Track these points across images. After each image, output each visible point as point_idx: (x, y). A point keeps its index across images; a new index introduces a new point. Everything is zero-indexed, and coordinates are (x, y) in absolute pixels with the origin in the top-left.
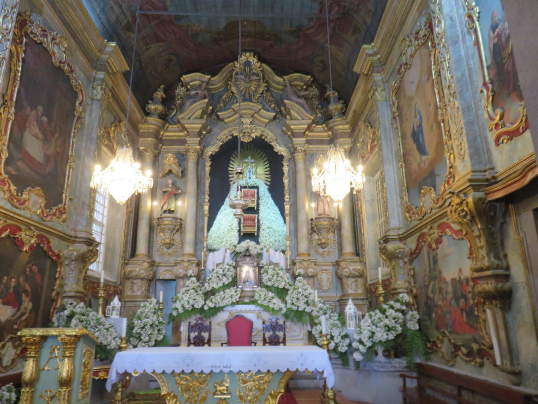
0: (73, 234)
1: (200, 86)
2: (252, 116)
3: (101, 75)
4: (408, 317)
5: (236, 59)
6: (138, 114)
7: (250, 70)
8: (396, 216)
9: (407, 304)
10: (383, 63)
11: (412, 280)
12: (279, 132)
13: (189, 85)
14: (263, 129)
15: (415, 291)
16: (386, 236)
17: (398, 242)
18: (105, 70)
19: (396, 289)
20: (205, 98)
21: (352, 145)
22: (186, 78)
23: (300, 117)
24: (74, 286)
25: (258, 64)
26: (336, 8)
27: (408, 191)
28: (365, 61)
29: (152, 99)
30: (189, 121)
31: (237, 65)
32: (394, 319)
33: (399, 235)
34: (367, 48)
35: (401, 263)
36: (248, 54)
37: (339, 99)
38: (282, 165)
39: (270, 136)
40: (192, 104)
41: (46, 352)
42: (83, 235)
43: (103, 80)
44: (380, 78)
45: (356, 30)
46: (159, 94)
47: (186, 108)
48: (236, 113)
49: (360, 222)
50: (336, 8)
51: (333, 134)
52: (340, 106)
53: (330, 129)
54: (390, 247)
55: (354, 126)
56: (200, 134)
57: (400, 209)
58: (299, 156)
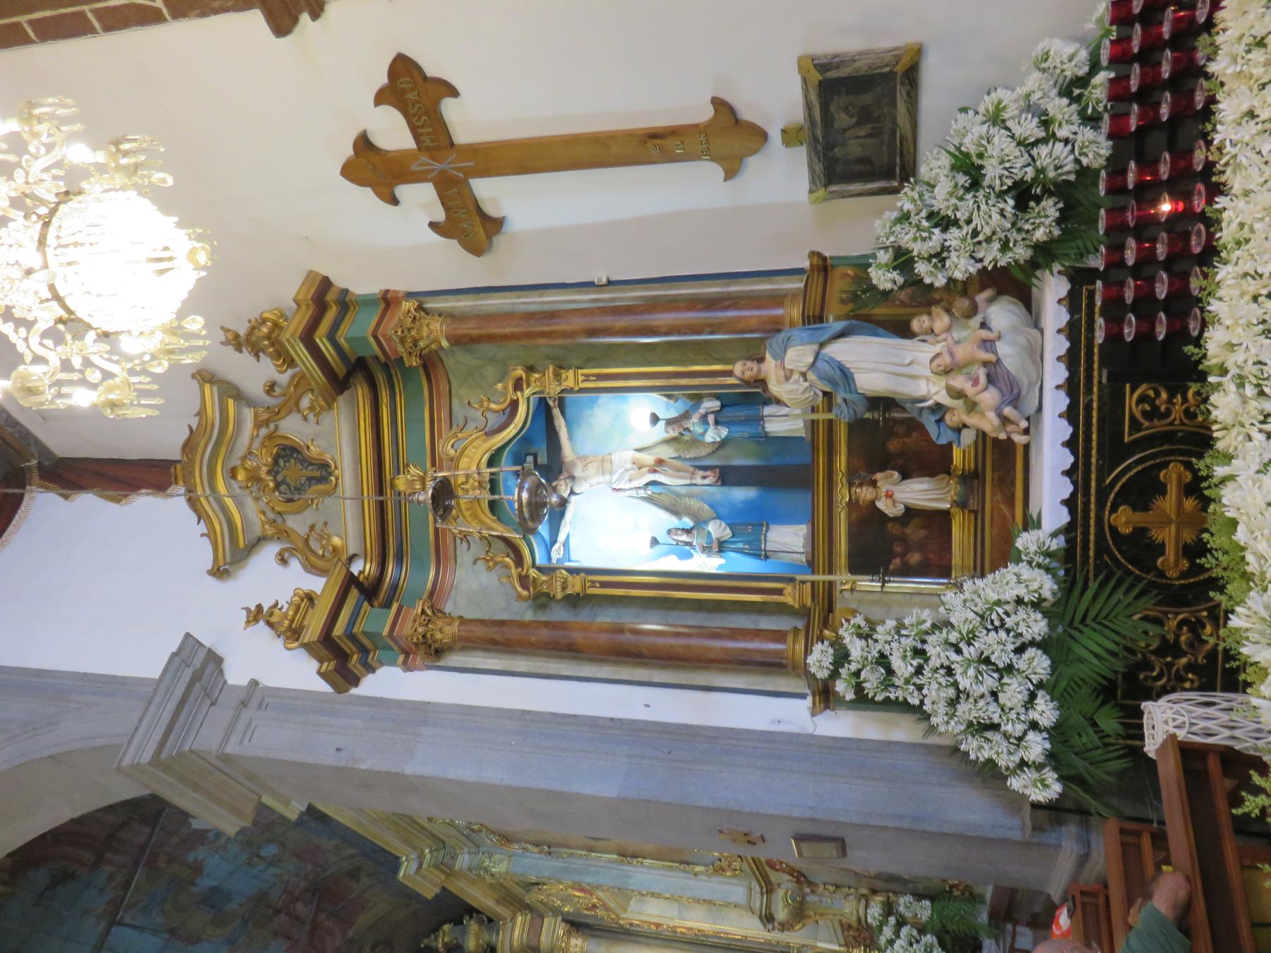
4: (908, 915)
8: (726, 887)
9: (889, 909)
10: (440, 843)
11: (846, 890)
15: (864, 891)
16: (761, 918)
17: (774, 896)
19: (859, 920)
21: (560, 918)
26: (300, 908)
27: (688, 863)
28: (424, 877)
32: (911, 945)
33: (762, 894)
34: (406, 871)
35: (811, 898)
37: (458, 922)
44: (467, 856)
45: (354, 874)
49: (719, 938)
50: (300, 908)
52: (473, 927)
54: (781, 914)
55: (529, 908)
57: (715, 879)
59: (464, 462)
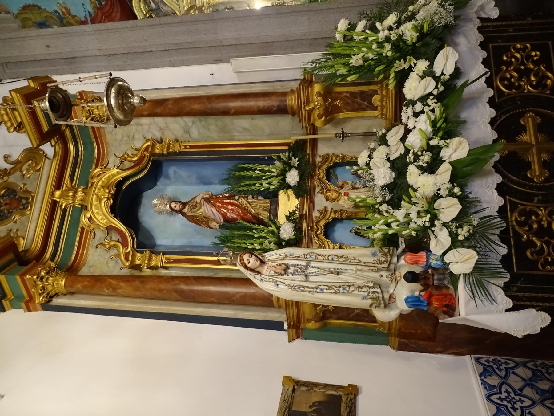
13: (146, 15)
30: (181, 4)
40: (165, 4)
47: (170, 9)
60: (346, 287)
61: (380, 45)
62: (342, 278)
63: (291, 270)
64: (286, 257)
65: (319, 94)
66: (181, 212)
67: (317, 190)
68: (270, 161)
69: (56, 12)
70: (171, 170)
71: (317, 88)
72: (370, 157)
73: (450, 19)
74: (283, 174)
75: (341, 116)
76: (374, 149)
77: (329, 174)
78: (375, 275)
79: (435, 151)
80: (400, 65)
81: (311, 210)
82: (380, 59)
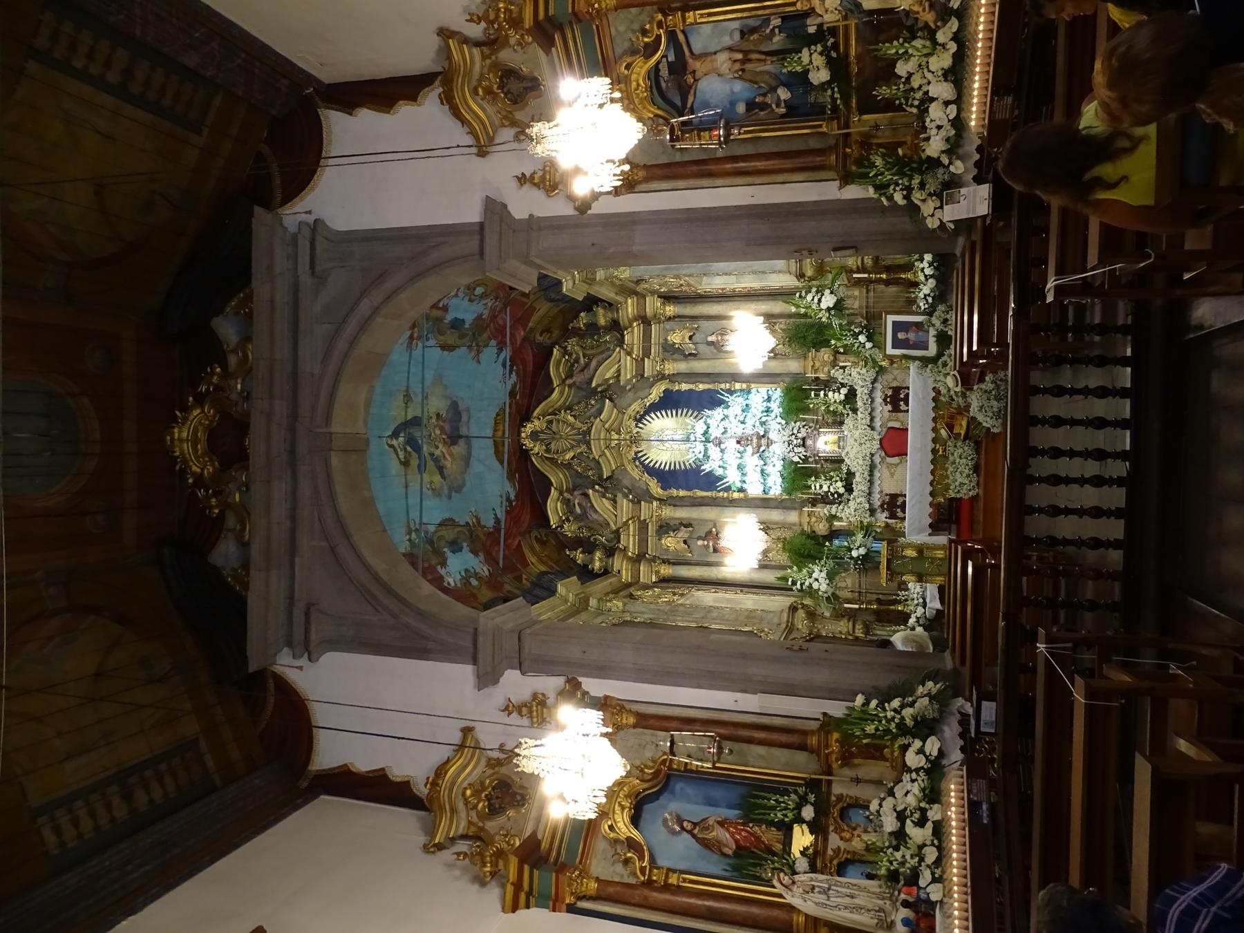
0: (784, 626)
1: (567, 502)
2: (607, 430)
3: (593, 602)
5: (527, 451)
6: (613, 579)
7: (542, 432)
12: (631, 394)
14: (626, 417)
18: (587, 601)
20: (586, 495)
22: (553, 522)
23: (618, 366)
24: (842, 623)
25: (536, 422)
29: (586, 566)
31: (536, 450)
34: (566, 288)
36: (523, 435)
38: (679, 391)
39: (636, 407)
40: (596, 511)
41: (898, 570)
42: (785, 616)
43: (600, 600)
46: (580, 557)
48: (603, 454)
51: (636, 319)
52: (601, 311)
53: (631, 326)
54: (809, 272)
55: (636, 293)
56: (637, 502)
58: (670, 368)
59: (634, 77)
60: (859, 909)
61: (888, 721)
62: (856, 901)
63: (817, 890)
64: (812, 880)
65: (837, 741)
66: (690, 832)
67: (831, 828)
68: (785, 793)
69: (468, 524)
70: (678, 786)
71: (836, 736)
72: (880, 805)
73: (936, 715)
74: (799, 807)
75: (856, 761)
76: (884, 799)
77: (843, 814)
78: (881, 902)
79: (923, 811)
80: (902, 741)
81: (825, 848)
82: (887, 731)
